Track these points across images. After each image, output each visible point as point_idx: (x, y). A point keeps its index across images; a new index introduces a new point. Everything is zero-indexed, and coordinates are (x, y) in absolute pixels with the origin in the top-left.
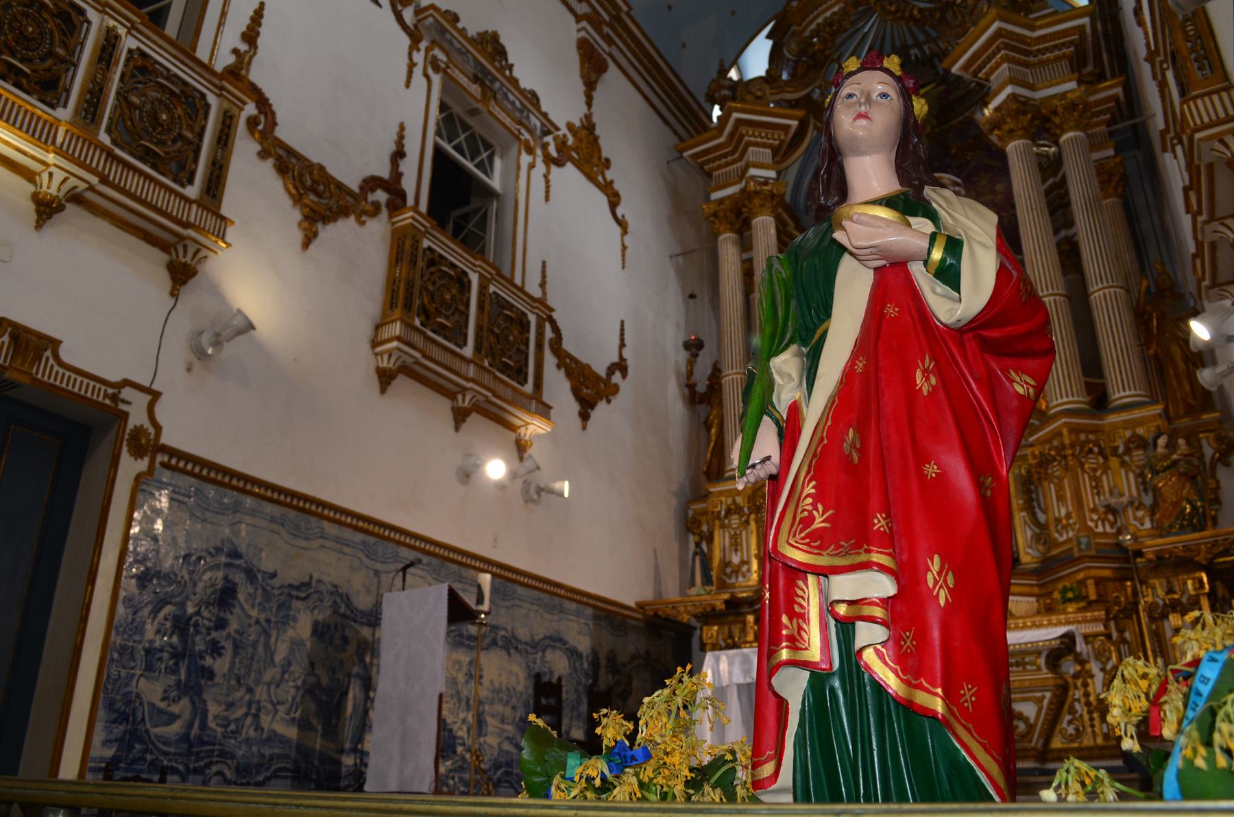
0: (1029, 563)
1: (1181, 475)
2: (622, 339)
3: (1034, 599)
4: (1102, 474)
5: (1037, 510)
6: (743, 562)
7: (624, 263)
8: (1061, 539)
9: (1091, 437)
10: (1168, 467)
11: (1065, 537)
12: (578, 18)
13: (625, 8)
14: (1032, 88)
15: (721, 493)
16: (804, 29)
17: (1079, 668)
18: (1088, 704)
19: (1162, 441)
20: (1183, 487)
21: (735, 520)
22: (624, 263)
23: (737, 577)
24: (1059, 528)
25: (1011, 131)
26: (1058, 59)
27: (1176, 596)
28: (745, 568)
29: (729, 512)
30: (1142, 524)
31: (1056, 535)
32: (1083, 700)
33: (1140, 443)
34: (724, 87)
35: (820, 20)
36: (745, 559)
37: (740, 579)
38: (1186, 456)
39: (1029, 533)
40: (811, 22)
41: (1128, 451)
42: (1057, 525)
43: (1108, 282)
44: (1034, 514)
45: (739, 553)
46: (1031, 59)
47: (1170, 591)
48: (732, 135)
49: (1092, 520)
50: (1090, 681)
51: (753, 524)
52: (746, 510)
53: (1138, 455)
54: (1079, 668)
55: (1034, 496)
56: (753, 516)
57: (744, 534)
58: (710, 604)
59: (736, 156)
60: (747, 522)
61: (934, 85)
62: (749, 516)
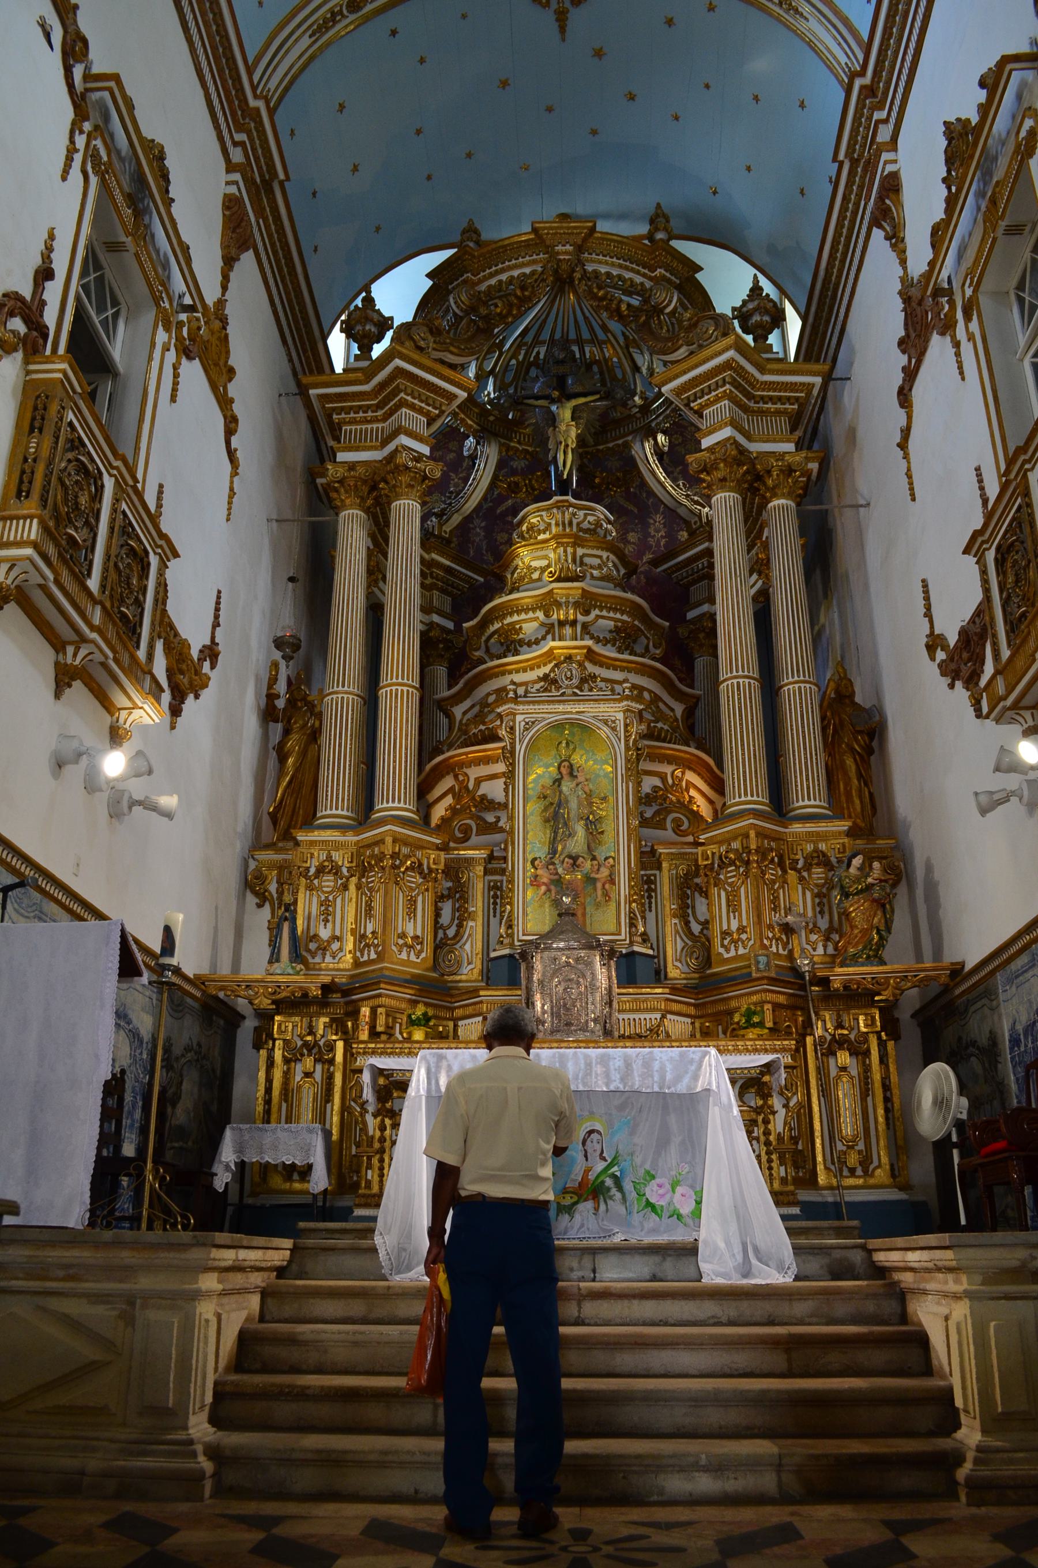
0: (676, 979)
1: (874, 901)
2: (217, 617)
3: (689, 1020)
4: (779, 888)
5: (691, 918)
6: (335, 938)
7: (229, 514)
8: (726, 956)
10: (862, 891)
11: (732, 953)
14: (749, 438)
15: (312, 843)
16: (480, 281)
17: (760, 1102)
18: (768, 1143)
19: (857, 861)
20: (875, 915)
21: (328, 882)
22: (229, 514)
24: (726, 942)
25: (723, 480)
26: (778, 412)
27: (846, 1032)
28: (335, 946)
29: (320, 871)
30: (814, 950)
31: (721, 950)
32: (762, 1138)
33: (821, 859)
34: (372, 321)
35: (504, 277)
36: (338, 933)
37: (328, 959)
38: (881, 881)
39: (680, 944)
40: (492, 275)
41: (808, 867)
42: (723, 939)
43: (804, 676)
44: (687, 923)
45: (329, 925)
46: (752, 404)
47: (840, 1026)
48: (382, 386)
49: (768, 938)
50: (771, 1117)
51: (352, 887)
52: (345, 870)
54: (760, 1102)
55: (689, 902)
56: (354, 880)
57: (339, 901)
58: (300, 988)
60: (345, 887)
61: (597, 396)
62: (348, 879)
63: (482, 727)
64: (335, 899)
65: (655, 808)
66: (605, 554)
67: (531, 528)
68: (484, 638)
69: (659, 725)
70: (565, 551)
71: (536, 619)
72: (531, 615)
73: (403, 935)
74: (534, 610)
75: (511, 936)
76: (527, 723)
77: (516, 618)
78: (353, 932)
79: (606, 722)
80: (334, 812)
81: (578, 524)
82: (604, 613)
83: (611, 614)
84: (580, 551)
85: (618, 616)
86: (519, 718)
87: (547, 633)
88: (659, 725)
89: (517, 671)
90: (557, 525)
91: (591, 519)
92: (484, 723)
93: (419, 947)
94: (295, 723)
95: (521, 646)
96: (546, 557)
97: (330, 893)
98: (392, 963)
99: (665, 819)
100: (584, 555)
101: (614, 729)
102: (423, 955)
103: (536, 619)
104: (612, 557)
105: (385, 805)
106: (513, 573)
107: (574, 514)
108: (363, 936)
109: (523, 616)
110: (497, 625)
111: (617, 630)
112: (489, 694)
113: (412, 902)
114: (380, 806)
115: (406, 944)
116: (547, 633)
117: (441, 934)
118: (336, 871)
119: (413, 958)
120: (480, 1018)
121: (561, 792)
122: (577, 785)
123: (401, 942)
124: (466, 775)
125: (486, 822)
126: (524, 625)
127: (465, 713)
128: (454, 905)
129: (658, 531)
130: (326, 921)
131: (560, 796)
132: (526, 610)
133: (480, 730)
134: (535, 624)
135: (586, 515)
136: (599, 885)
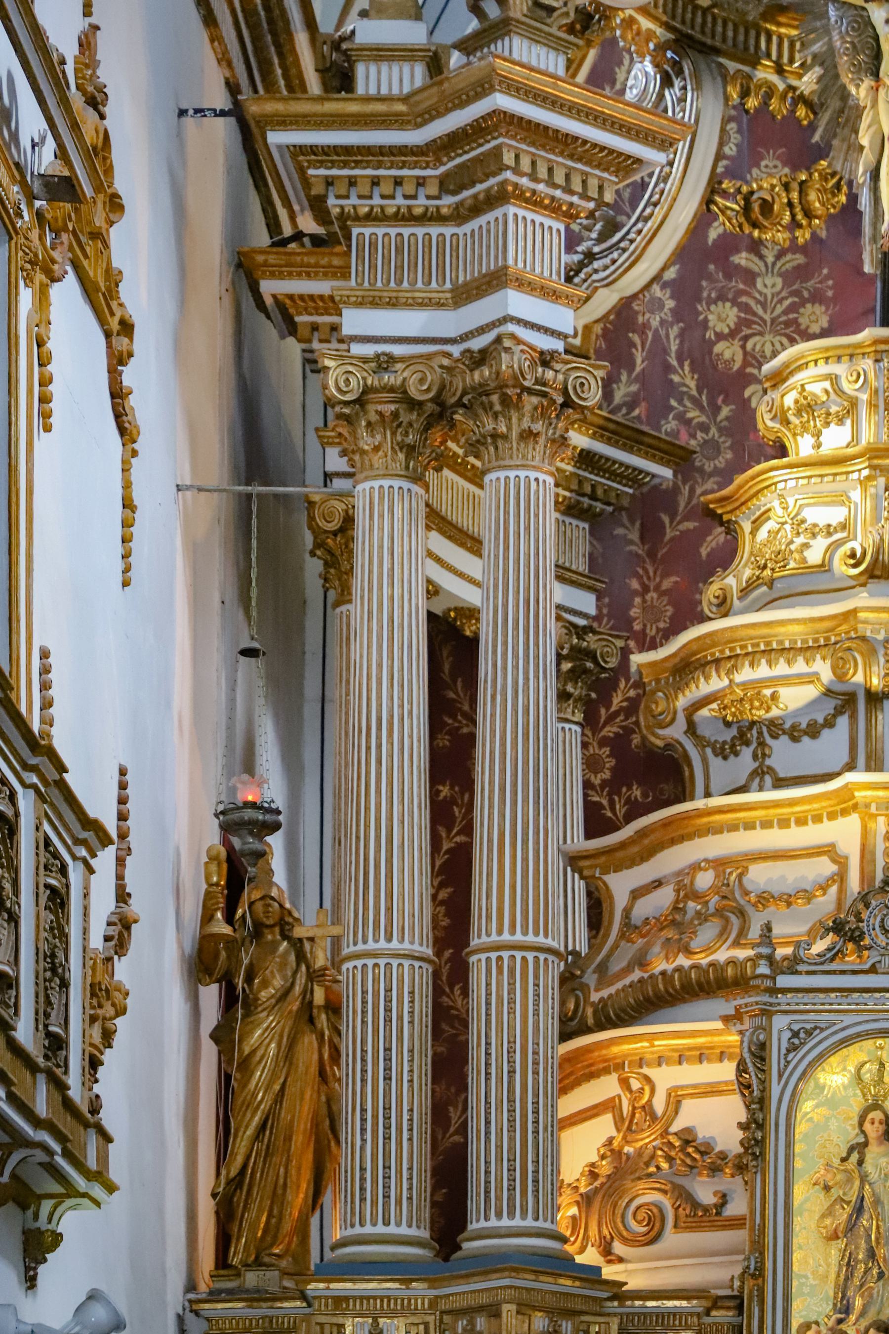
63: (683, 961)
68: (682, 701)
71: (812, 678)
72: (800, 666)
74: (807, 651)
76: (796, 1034)
77: (763, 671)
86: (780, 1022)
92: (688, 952)
95: (775, 737)
96: (841, 499)
103: (812, 678)
106: (757, 524)
109: (782, 668)
110: (715, 683)
112: (696, 867)
121: (864, 1179)
124: (648, 1079)
127: (637, 894)
131: (862, 1188)
132: (789, 652)
133: (678, 969)
134: (810, 692)
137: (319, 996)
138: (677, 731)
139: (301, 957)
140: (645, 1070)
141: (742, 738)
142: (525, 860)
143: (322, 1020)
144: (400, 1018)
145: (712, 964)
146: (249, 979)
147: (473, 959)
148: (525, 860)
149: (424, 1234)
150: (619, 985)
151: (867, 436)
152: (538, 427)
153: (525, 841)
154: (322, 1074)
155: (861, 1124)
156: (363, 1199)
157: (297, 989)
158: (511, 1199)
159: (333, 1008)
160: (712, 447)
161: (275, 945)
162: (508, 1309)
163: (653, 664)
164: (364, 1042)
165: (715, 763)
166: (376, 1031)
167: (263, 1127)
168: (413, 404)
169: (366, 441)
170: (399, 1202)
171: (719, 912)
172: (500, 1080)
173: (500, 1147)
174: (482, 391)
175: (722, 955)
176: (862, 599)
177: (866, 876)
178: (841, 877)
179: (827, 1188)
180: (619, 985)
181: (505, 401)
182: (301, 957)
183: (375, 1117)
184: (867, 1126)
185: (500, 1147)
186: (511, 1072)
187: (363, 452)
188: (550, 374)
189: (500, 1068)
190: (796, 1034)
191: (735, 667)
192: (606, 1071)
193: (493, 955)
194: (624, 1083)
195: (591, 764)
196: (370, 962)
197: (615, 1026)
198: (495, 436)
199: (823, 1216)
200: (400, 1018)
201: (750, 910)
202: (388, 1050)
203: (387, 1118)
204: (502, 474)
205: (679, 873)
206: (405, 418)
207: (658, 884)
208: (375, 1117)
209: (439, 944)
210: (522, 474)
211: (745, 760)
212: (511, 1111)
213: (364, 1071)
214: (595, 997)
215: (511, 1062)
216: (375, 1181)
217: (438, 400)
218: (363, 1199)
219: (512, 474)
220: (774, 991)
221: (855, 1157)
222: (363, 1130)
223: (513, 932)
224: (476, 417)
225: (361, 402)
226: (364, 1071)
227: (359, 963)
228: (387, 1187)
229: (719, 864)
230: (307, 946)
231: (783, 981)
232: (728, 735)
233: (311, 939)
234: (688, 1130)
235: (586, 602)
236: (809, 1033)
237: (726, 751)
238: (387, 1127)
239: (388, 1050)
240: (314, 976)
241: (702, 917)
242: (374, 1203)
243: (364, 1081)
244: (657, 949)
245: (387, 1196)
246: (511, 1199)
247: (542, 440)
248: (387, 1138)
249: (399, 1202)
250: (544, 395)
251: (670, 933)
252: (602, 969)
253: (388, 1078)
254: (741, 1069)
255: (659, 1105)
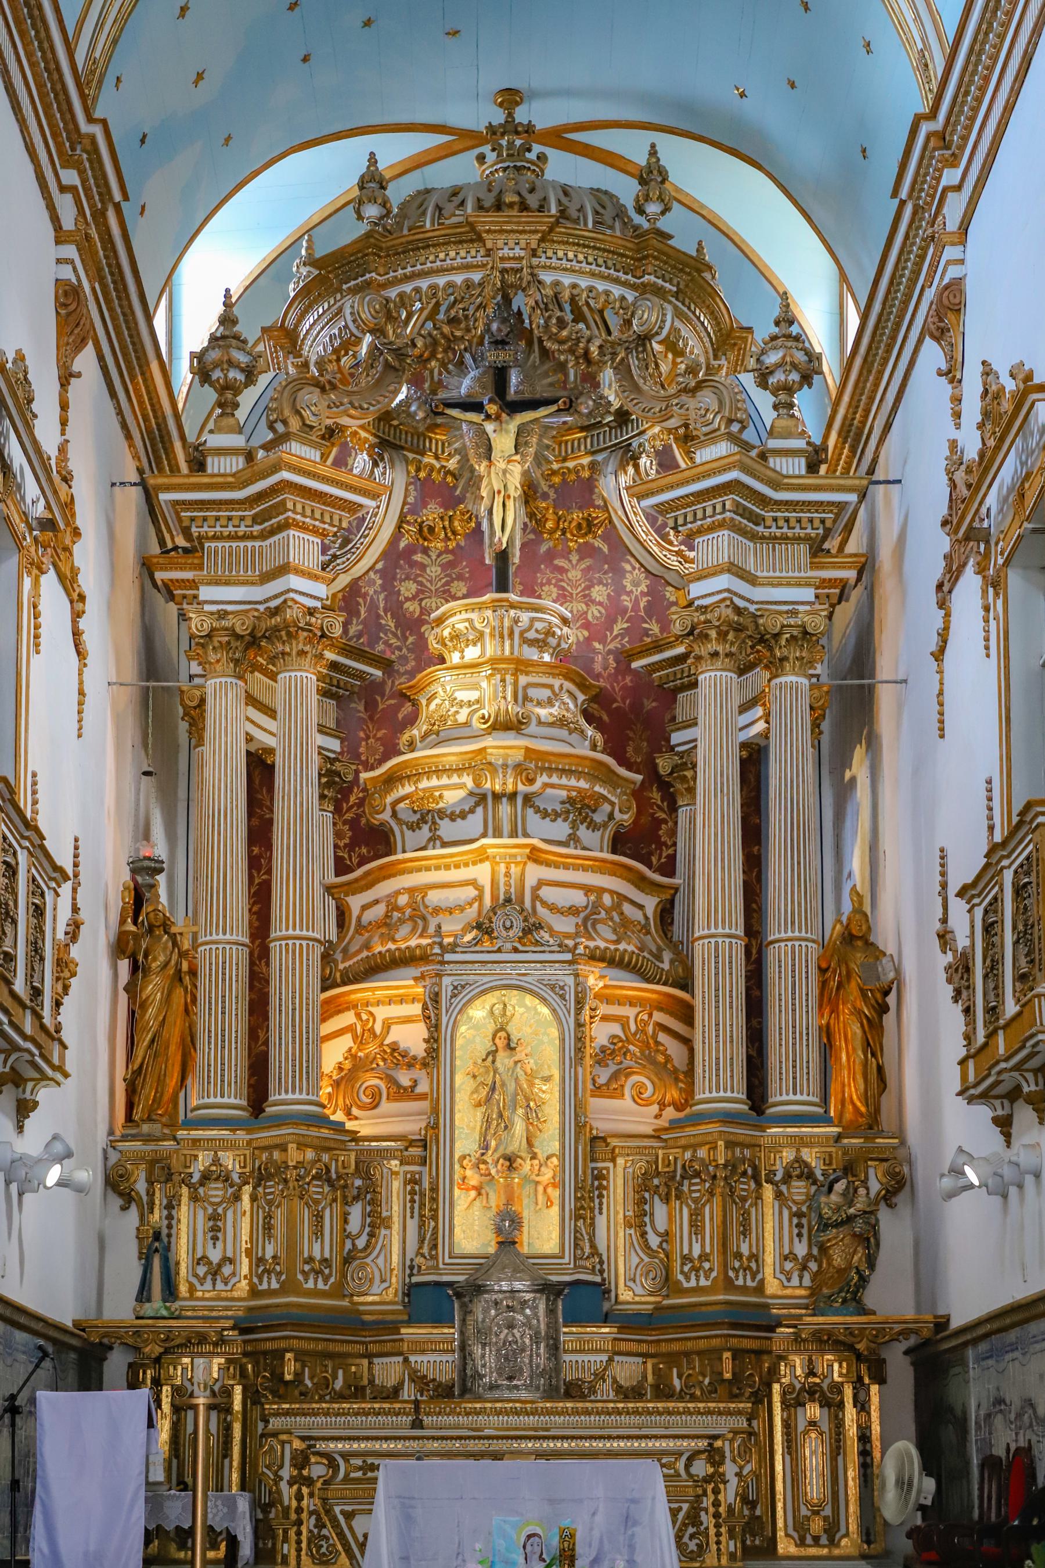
9: (747, 1153)
12: (61, 237)
13: (117, 196)
21: (216, 1191)
23: (214, 1281)
25: (715, 654)
28: (227, 1270)
33: (803, 1171)
36: (229, 1254)
39: (635, 1260)
41: (788, 1178)
44: (644, 1234)
45: (220, 1244)
53: (799, 1189)
56: (247, 1189)
57: (230, 1214)
59: (257, 528)
60: (237, 1198)
63: (391, 946)
64: (225, 1210)
65: (613, 1068)
66: (557, 683)
67: (456, 636)
68: (389, 799)
69: (622, 946)
70: (503, 680)
72: (455, 779)
73: (310, 1260)
74: (459, 770)
75: (434, 1258)
76: (455, 988)
77: (434, 782)
78: (249, 1253)
79: (553, 988)
80: (219, 1100)
81: (522, 633)
82: (555, 779)
83: (564, 781)
84: (523, 680)
85: (573, 782)
86: (446, 981)
87: (477, 804)
88: (622, 946)
89: (438, 868)
90: (492, 635)
91: (539, 625)
92: (394, 941)
93: (327, 1271)
94: (155, 959)
96: (476, 687)
97: (219, 1204)
98: (298, 1295)
99: (622, 1086)
100: (529, 685)
101: (562, 997)
102: (332, 1280)
104: (568, 685)
105: (283, 1096)
106: (430, 700)
107: (516, 621)
108: (261, 1260)
109: (445, 781)
110: (408, 789)
111: (571, 801)
112: (398, 893)
113: (319, 1217)
114: (277, 1097)
115: (313, 1270)
116: (477, 804)
117: (348, 1245)
118: (226, 1178)
119: (321, 1285)
120: (400, 1359)
122: (516, 1063)
123: (307, 1268)
124: (371, 1014)
125: (399, 1086)
126: (446, 793)
127: (365, 908)
128: (364, 1209)
129: (636, 584)
130: (215, 1239)
132: (448, 771)
133: (388, 951)
135: (532, 620)
136: (540, 1189)
137: (185, 966)
138: (386, 816)
139: (175, 944)
140: (370, 1009)
141: (423, 820)
142: (301, 888)
143: (187, 979)
144: (231, 978)
145: (407, 948)
146: (146, 956)
147: (272, 945)
148: (301, 888)
149: (244, 1103)
150: (355, 960)
151: (489, 652)
152: (307, 648)
153: (301, 878)
154: (187, 1011)
155: (493, 1039)
156: (209, 1083)
157: (173, 962)
158: (294, 1083)
159: (193, 973)
160: (404, 659)
161: (160, 937)
162: (292, 1147)
163: (373, 778)
164: (210, 992)
165: (408, 833)
166: (217, 986)
167: (152, 1041)
168: (238, 637)
169: (212, 657)
170: (229, 1085)
171: (411, 918)
172: (287, 1014)
173: (287, 1053)
174: (276, 629)
175: (413, 943)
176: (489, 742)
177: (494, 897)
178: (480, 898)
179: (474, 1077)
180: (355, 960)
181: (289, 634)
182: (175, 944)
183: (216, 1035)
184: (497, 1041)
185: (287, 1053)
186: (294, 1009)
187: (211, 663)
188: (313, 620)
189: (287, 1007)
190: (455, 988)
191: (418, 780)
192: (348, 1009)
193: (283, 943)
194: (358, 1016)
195: (338, 835)
196: (214, 947)
197: (352, 983)
198: (283, 653)
199: (473, 1093)
200: (231, 978)
201: (429, 917)
202: (224, 996)
203: (223, 1036)
204: (287, 674)
205: (388, 896)
206: (233, 644)
207: (377, 902)
208: (216, 1035)
209: (253, 937)
210: (299, 674)
211: (425, 832)
212: (294, 1032)
213: (210, 1009)
214: (341, 966)
215: (294, 1004)
216: (216, 1072)
217: (252, 634)
218: (209, 1083)
219: (293, 674)
220: (443, 963)
221: (490, 1058)
222: (209, 1043)
223: (294, 929)
224: (273, 644)
225: (209, 636)
226: (210, 1009)
227: (208, 947)
228: (222, 1075)
229: (411, 891)
230: (179, 937)
231: (448, 957)
232: (415, 818)
233: (181, 934)
234: (395, 1043)
235: (335, 745)
236: (463, 987)
237: (413, 827)
238: (223, 1041)
239: (224, 996)
240: (183, 955)
241: (402, 921)
242: (215, 1085)
243: (210, 1014)
244: (376, 939)
245: (222, 1081)
246: (294, 1083)
247: (309, 655)
248: (223, 1047)
249: (229, 1085)
250: (310, 631)
251: (383, 930)
252: (345, 951)
253: (223, 1013)
254: (425, 1008)
255: (378, 1029)
